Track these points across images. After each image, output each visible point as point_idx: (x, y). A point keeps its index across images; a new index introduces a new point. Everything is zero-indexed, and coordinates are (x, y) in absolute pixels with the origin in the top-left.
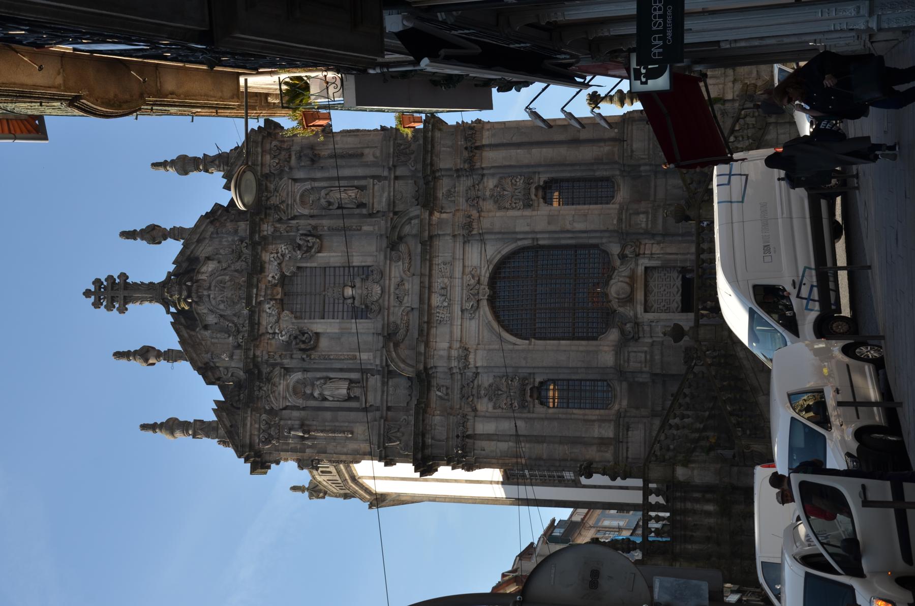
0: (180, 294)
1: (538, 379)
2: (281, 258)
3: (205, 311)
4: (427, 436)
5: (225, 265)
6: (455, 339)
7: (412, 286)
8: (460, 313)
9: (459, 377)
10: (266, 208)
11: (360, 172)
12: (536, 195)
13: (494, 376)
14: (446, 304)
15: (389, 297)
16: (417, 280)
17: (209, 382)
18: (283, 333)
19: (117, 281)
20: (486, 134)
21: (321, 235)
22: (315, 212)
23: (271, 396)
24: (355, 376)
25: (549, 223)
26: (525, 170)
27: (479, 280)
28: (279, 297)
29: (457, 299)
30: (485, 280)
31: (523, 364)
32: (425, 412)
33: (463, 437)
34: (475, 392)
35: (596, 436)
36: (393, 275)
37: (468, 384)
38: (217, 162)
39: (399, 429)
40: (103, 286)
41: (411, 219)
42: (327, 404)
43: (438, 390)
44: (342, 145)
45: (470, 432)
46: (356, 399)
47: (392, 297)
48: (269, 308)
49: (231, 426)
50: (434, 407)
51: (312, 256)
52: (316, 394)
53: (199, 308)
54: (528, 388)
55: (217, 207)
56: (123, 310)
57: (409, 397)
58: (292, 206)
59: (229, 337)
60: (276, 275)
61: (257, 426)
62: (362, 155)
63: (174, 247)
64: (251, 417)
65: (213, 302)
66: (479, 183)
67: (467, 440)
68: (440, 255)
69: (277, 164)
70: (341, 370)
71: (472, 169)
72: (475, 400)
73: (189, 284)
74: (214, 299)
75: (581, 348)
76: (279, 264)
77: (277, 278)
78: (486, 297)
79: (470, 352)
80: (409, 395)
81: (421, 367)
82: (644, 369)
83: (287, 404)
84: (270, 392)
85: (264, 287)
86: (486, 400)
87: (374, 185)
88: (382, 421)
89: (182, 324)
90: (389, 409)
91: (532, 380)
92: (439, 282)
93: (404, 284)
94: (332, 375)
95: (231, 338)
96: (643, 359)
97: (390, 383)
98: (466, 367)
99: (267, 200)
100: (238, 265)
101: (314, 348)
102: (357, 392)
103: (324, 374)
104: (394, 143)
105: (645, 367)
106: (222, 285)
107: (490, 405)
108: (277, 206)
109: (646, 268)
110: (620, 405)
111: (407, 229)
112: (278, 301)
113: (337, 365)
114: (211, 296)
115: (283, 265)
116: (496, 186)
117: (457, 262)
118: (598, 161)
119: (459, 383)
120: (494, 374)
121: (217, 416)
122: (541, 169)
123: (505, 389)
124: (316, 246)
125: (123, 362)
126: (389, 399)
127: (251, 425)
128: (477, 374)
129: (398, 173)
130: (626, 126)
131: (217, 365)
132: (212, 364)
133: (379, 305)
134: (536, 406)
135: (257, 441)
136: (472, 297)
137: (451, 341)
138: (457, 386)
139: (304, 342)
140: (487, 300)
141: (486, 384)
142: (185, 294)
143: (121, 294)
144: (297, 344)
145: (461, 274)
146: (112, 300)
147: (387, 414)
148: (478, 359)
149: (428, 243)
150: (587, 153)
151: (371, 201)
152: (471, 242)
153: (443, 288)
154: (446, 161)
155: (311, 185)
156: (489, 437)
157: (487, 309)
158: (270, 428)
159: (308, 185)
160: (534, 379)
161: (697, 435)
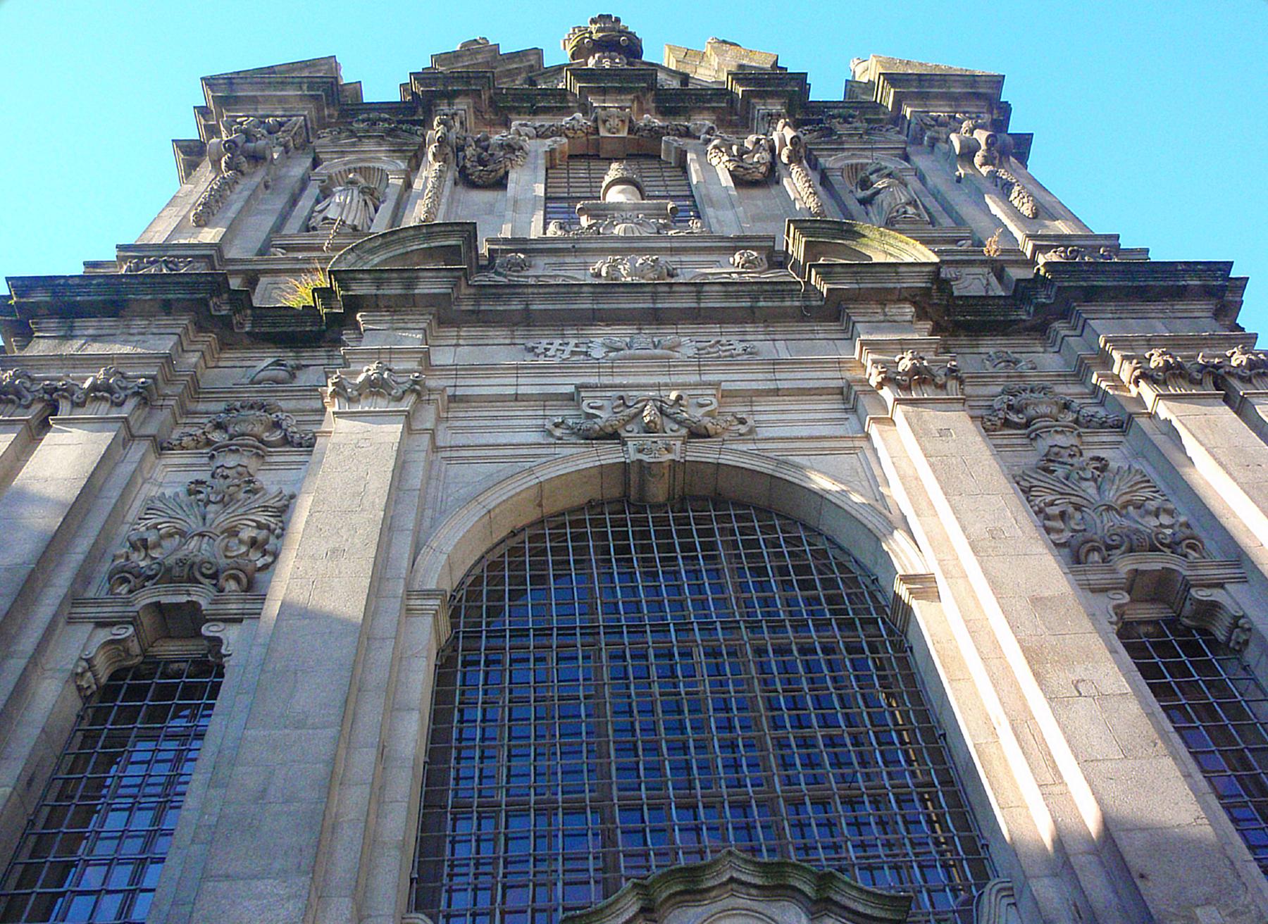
1: (231, 635)
4: (108, 322)
6: (460, 382)
12: (1134, 583)
30: (703, 453)
37: (277, 425)
42: (305, 204)
43: (277, 363)
50: (221, 364)
54: (202, 596)
69: (936, 119)
75: (353, 800)
78: (633, 456)
79: (399, 399)
91: (233, 608)
116: (1102, 465)
117: (761, 376)
137: (456, 370)
145: (724, 386)
152: (853, 418)
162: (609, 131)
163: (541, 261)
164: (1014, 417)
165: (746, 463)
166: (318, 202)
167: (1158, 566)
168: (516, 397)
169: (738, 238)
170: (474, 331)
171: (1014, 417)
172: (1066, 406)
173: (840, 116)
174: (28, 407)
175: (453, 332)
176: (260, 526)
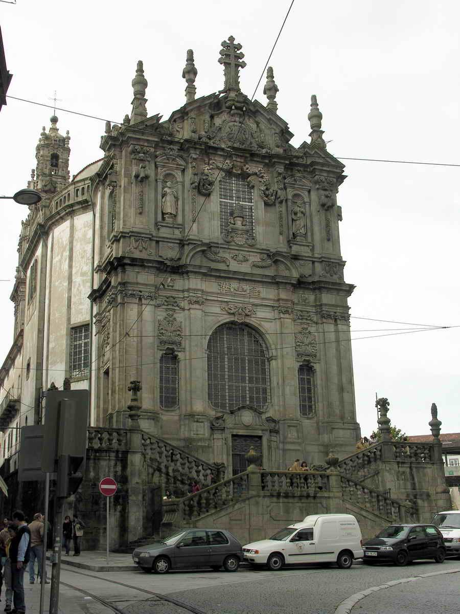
0: (237, 102)
1: (180, 355)
2: (261, 175)
3: (223, 118)
5: (255, 135)
7: (245, 268)
8: (226, 300)
9: (182, 297)
10: (292, 169)
11: (317, 237)
13: (182, 322)
14: (232, 290)
15: (237, 250)
16: (248, 270)
17: (174, 113)
18: (210, 171)
19: (241, 61)
20: (345, 328)
21: (275, 205)
22: (290, 203)
23: (165, 157)
24: (180, 219)
25: (288, 368)
26: (322, 353)
27: (248, 315)
28: (234, 171)
29: (235, 298)
30: (247, 320)
31: (193, 344)
32: (158, 269)
33: (141, 296)
34: (170, 307)
35: (143, 395)
36: (251, 254)
37: (176, 302)
38: (319, 140)
39: (144, 248)
40: (236, 50)
41: (289, 269)
43: (171, 280)
44: (332, 225)
45: (144, 301)
46: (163, 219)
47: (236, 252)
48: (227, 163)
49: (146, 125)
51: (262, 198)
52: (166, 189)
53: (226, 113)
55: (292, 135)
56: (220, 61)
57: (165, 258)
58: (294, 188)
59: (206, 132)
60: (249, 170)
61: (146, 144)
62: (329, 240)
63: (264, 101)
64: (154, 141)
65: (232, 124)
66: (312, 321)
67: (138, 299)
68: (265, 289)
70: (183, 210)
71: (323, 317)
72: (164, 307)
73: (244, 109)
74: (234, 125)
76: (256, 174)
77: (248, 171)
78: (236, 320)
79: (200, 305)
80: (167, 258)
81: (190, 269)
82: (192, 433)
83: (159, 168)
84: (168, 156)
85: (242, 161)
86: (165, 314)
87: (308, 246)
88: (151, 237)
89: (214, 100)
90: (157, 242)
91: (180, 350)
92: (247, 287)
93: (245, 261)
94: (180, 203)
95: (204, 133)
96: (199, 433)
97: (176, 245)
98: (190, 303)
99: (298, 170)
100: (254, 145)
101: (200, 193)
102: (169, 220)
103: (180, 198)
104: (337, 263)
105: (194, 434)
106: (243, 132)
107: (161, 318)
108: (294, 177)
109: (260, 437)
110: (162, 414)
111: (282, 267)
112: (231, 170)
113: (187, 208)
114: (235, 123)
115: (255, 177)
116: (310, 333)
118: (330, 405)
119: (177, 296)
120: (183, 321)
121: (152, 118)
122: (323, 363)
123: (173, 329)
124: (269, 201)
125: (185, 57)
126: (165, 243)
127: (148, 140)
128: (183, 309)
129: (317, 264)
130: (353, 425)
131: (186, 121)
132: (186, 118)
133: (231, 242)
134: (161, 351)
135: (135, 143)
136: (237, 309)
138: (174, 294)
139: (204, 185)
140: (234, 321)
141: (175, 316)
142: (238, 105)
143: (233, 62)
144: (204, 179)
146: (228, 56)
147: (154, 240)
148: (196, 313)
149: (275, 282)
150: (335, 397)
151: (298, 243)
153: (243, 289)
154: (327, 298)
155: (307, 202)
156: (140, 314)
157: (228, 320)
158: (144, 153)
159: (306, 200)
160: (180, 352)
161: (164, 470)
162: (236, 170)
163: (221, 250)
164: (300, 318)
165: (254, 324)
166: (162, 198)
167: (308, 359)
168: (217, 300)
169: (262, 249)
170: (209, 278)
171: (300, 318)
172: (310, 316)
173: (298, 170)
174: (136, 298)
175: (205, 277)
176: (179, 330)
